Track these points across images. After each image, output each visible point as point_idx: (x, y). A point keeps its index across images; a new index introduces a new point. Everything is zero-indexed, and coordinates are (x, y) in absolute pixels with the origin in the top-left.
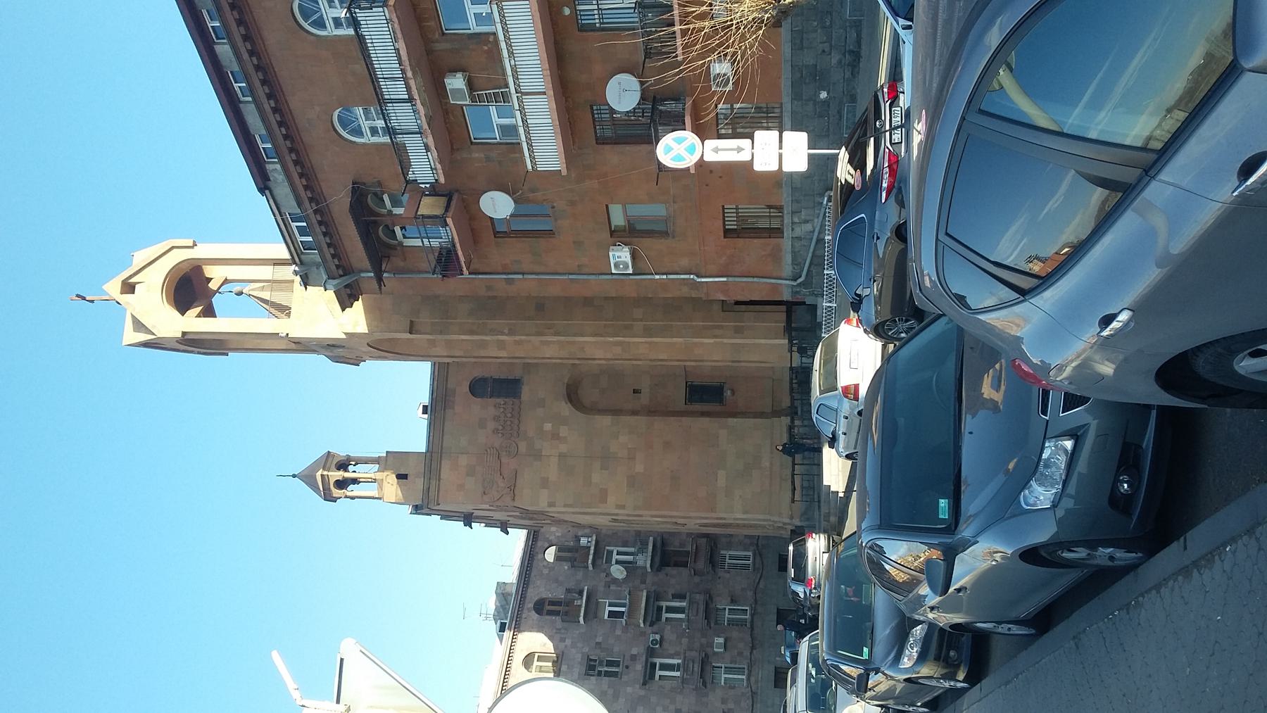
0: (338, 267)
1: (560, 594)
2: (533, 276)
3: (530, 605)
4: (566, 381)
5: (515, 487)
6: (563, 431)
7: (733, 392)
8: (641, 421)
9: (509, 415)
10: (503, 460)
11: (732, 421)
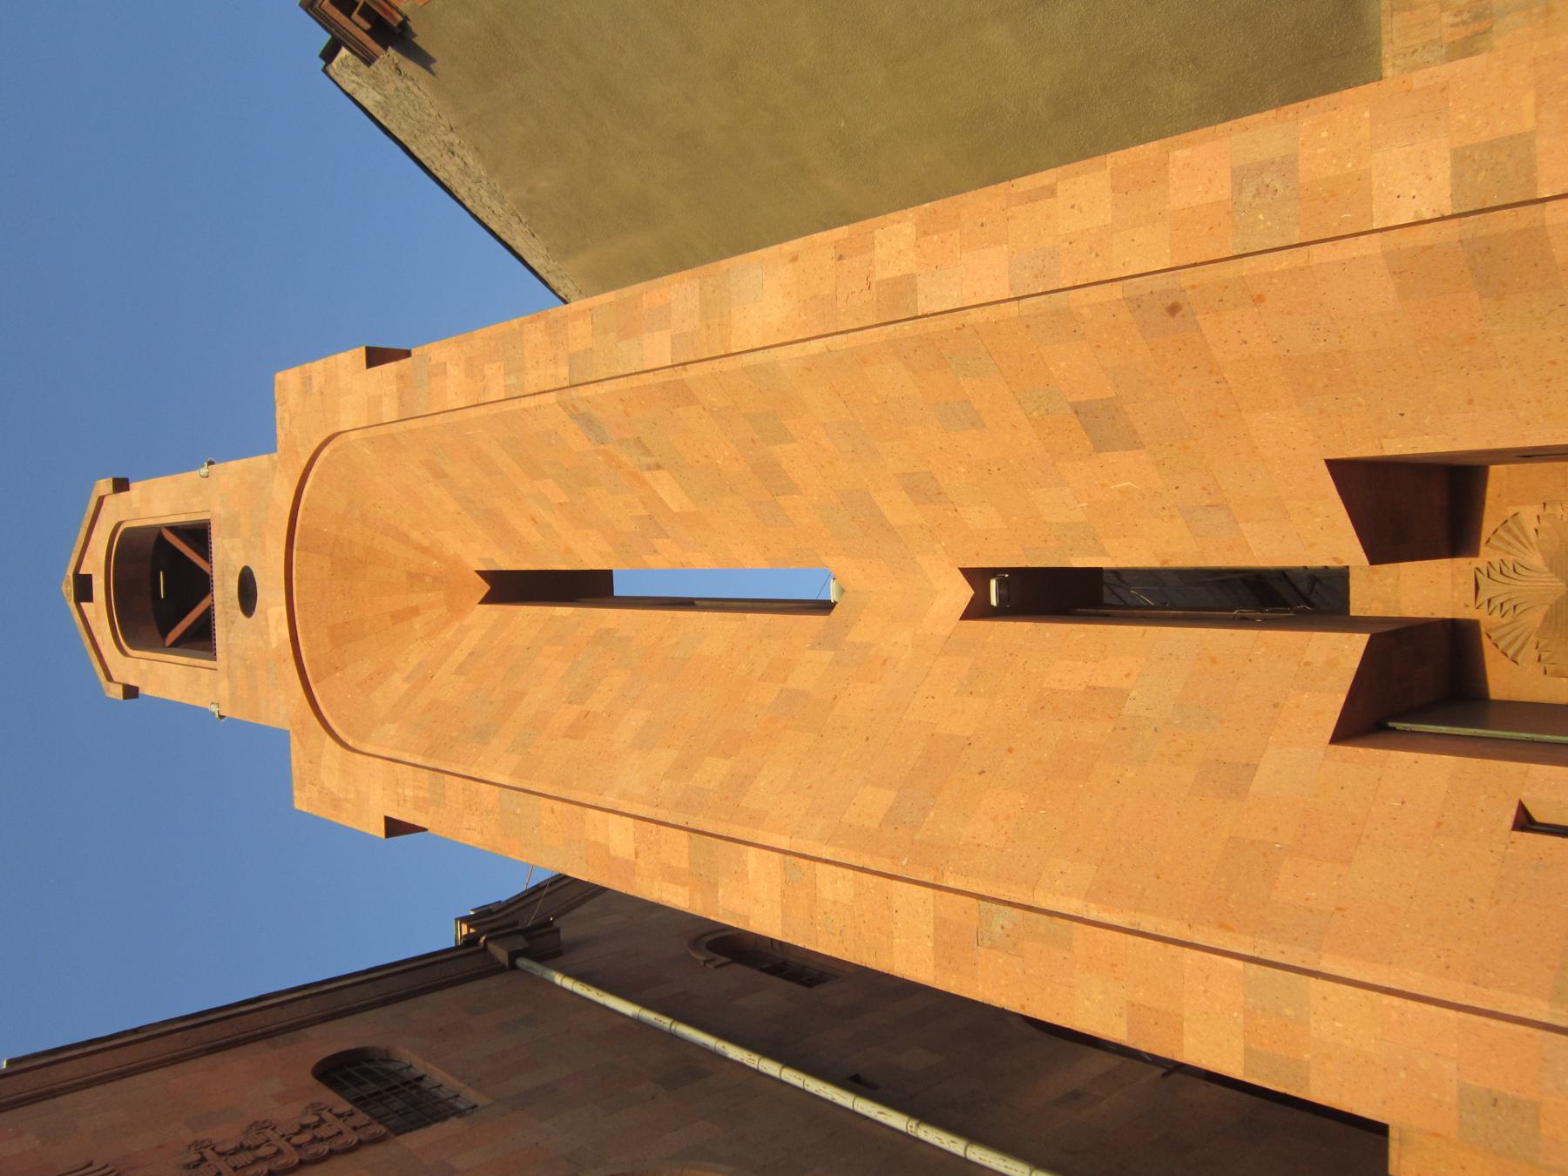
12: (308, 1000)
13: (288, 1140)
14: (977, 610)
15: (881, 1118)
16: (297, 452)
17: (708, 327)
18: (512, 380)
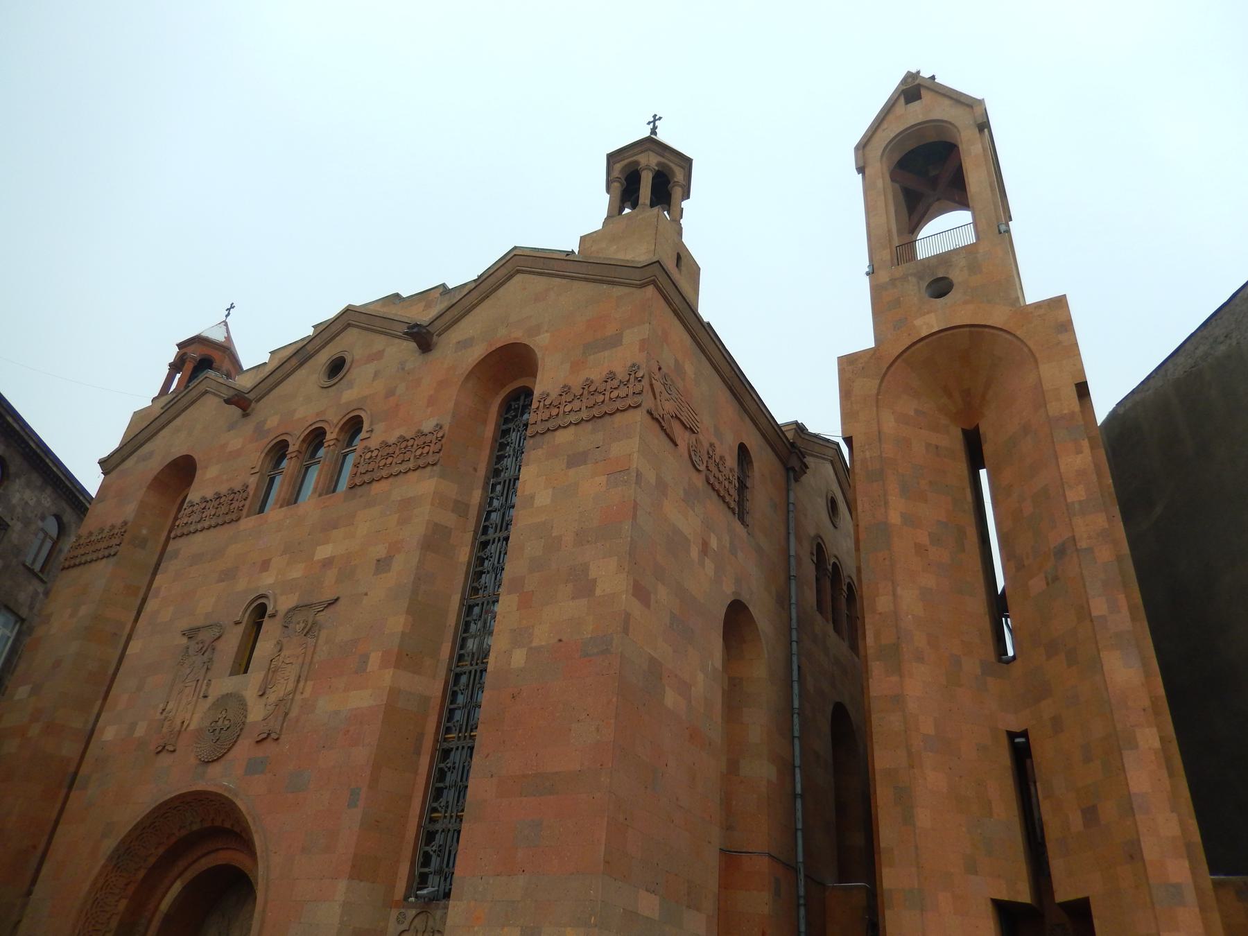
6: (709, 565)
10: (687, 434)
12: (757, 406)
14: (1012, 735)
15: (794, 696)
16: (1023, 326)
17: (1111, 637)
18: (1077, 506)
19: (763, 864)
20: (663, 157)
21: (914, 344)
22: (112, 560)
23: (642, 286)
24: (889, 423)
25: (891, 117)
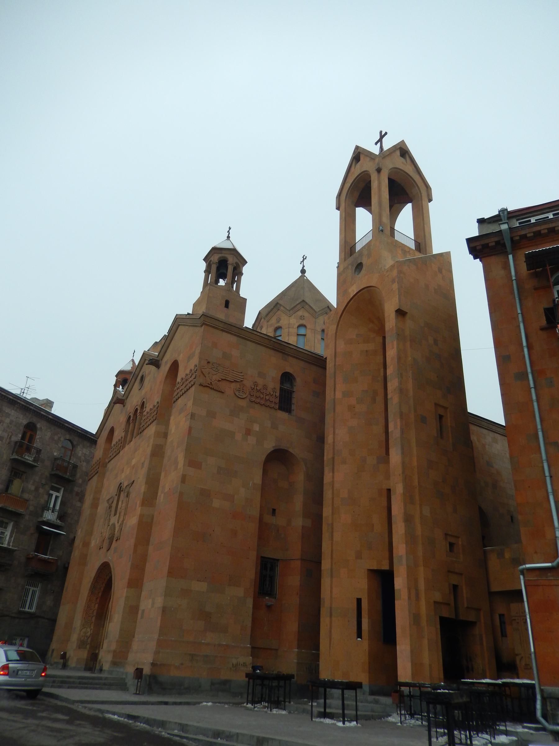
0: (524, 237)
1: (37, 444)
2: (534, 397)
3: (34, 420)
4: (291, 450)
5: (211, 388)
6: (252, 440)
7: (269, 607)
8: (255, 512)
9: (267, 397)
10: (233, 385)
11: (250, 602)
13: (266, 395)
19: (298, 563)
20: (222, 254)
21: (348, 303)
22: (97, 474)
23: (201, 326)
24: (341, 346)
25: (350, 175)
